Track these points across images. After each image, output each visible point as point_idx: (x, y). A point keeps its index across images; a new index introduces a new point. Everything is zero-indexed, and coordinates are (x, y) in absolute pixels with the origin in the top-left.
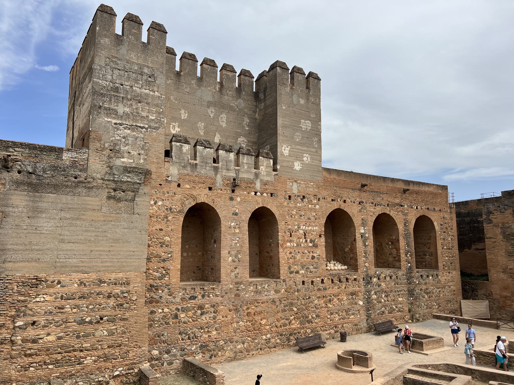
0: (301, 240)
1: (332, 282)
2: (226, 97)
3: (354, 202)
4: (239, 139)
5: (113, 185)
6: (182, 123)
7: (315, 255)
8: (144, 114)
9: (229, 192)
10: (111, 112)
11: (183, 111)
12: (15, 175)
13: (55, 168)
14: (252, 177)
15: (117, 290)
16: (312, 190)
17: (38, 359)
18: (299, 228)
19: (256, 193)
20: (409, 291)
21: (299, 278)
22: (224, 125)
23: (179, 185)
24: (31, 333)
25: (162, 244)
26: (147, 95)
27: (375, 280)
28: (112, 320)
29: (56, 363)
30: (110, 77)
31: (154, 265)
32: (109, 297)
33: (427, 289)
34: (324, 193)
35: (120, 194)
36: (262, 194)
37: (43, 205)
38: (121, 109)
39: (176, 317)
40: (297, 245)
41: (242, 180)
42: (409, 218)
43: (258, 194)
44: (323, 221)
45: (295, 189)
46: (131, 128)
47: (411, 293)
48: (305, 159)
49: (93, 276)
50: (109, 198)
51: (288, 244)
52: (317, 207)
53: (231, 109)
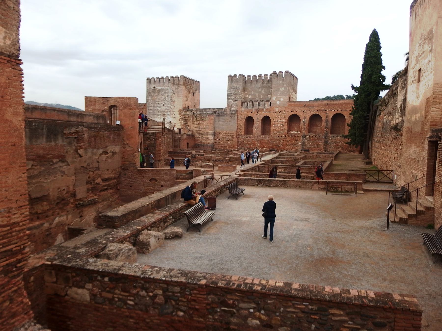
1: (289, 136)
2: (264, 84)
6: (252, 95)
9: (256, 113)
10: (230, 99)
12: (216, 114)
14: (263, 108)
15: (232, 135)
18: (278, 121)
20: (325, 141)
21: (276, 135)
22: (264, 93)
24: (219, 141)
25: (240, 126)
28: (231, 140)
29: (223, 147)
31: (239, 130)
34: (288, 110)
35: (232, 116)
37: (220, 119)
38: (232, 97)
39: (243, 141)
41: (260, 109)
42: (329, 115)
44: (287, 118)
45: (277, 109)
46: (234, 101)
47: (326, 142)
48: (281, 100)
49: (228, 132)
53: (266, 87)
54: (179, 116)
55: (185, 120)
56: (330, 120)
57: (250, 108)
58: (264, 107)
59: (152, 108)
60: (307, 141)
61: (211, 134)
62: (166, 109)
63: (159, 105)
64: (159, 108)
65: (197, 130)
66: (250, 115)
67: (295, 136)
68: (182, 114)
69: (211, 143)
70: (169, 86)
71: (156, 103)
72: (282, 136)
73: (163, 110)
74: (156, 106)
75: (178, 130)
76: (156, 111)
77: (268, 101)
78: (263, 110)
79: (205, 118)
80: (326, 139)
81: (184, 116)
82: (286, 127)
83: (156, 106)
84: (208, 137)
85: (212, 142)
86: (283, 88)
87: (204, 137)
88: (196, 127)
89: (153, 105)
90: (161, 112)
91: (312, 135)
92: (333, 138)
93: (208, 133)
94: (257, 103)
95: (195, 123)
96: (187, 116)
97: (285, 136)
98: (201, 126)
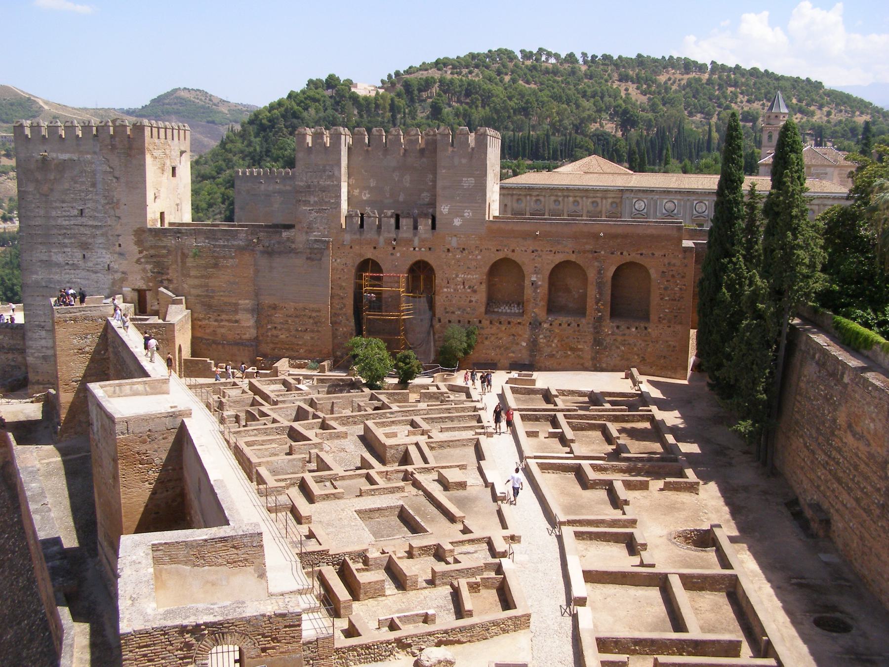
0: (459, 287)
1: (491, 323)
3: (526, 251)
4: (423, 195)
5: (308, 251)
7: (472, 299)
8: (327, 200)
9: (391, 248)
10: (307, 203)
11: (372, 180)
13: (279, 243)
15: (314, 314)
16: (473, 242)
17: (278, 346)
18: (457, 276)
19: (414, 249)
20: (595, 340)
23: (351, 247)
24: (275, 332)
25: (341, 287)
26: (329, 185)
27: (545, 326)
28: (312, 331)
30: (305, 179)
32: (310, 317)
33: (625, 340)
36: (420, 249)
38: (312, 199)
40: (455, 290)
43: (417, 249)
44: (486, 269)
45: (454, 242)
47: (597, 342)
48: (466, 214)
49: (301, 305)
50: (308, 259)
51: (445, 290)
52: (479, 257)
54: (135, 249)
55: (157, 264)
56: (610, 280)
57: (370, 234)
58: (415, 235)
59: (38, 221)
60: (545, 337)
61: (247, 310)
62: (92, 226)
63: (64, 213)
64: (67, 223)
65: (198, 296)
66: (369, 255)
67: (509, 323)
68: (147, 244)
69: (247, 336)
70: (95, 153)
71: (55, 205)
72: (469, 322)
73: (82, 229)
74: (54, 213)
75: (135, 295)
76: (55, 231)
77: (425, 216)
78: (409, 242)
79: (224, 257)
80: (598, 332)
81: (152, 252)
82: (481, 296)
83: (54, 213)
84: (237, 317)
85: (251, 333)
86: (472, 180)
87: (224, 317)
88: (195, 287)
89: (42, 212)
90: (74, 236)
91: (558, 322)
92: (616, 331)
93: (236, 304)
94: (393, 221)
95: (193, 273)
96: (165, 251)
97: (480, 322)
98: (213, 282)
